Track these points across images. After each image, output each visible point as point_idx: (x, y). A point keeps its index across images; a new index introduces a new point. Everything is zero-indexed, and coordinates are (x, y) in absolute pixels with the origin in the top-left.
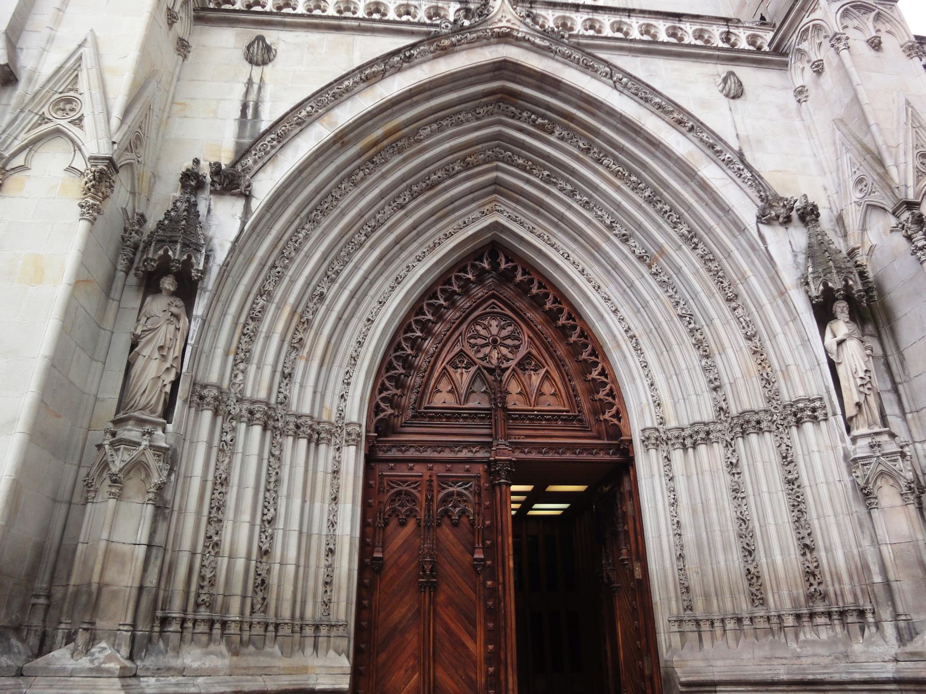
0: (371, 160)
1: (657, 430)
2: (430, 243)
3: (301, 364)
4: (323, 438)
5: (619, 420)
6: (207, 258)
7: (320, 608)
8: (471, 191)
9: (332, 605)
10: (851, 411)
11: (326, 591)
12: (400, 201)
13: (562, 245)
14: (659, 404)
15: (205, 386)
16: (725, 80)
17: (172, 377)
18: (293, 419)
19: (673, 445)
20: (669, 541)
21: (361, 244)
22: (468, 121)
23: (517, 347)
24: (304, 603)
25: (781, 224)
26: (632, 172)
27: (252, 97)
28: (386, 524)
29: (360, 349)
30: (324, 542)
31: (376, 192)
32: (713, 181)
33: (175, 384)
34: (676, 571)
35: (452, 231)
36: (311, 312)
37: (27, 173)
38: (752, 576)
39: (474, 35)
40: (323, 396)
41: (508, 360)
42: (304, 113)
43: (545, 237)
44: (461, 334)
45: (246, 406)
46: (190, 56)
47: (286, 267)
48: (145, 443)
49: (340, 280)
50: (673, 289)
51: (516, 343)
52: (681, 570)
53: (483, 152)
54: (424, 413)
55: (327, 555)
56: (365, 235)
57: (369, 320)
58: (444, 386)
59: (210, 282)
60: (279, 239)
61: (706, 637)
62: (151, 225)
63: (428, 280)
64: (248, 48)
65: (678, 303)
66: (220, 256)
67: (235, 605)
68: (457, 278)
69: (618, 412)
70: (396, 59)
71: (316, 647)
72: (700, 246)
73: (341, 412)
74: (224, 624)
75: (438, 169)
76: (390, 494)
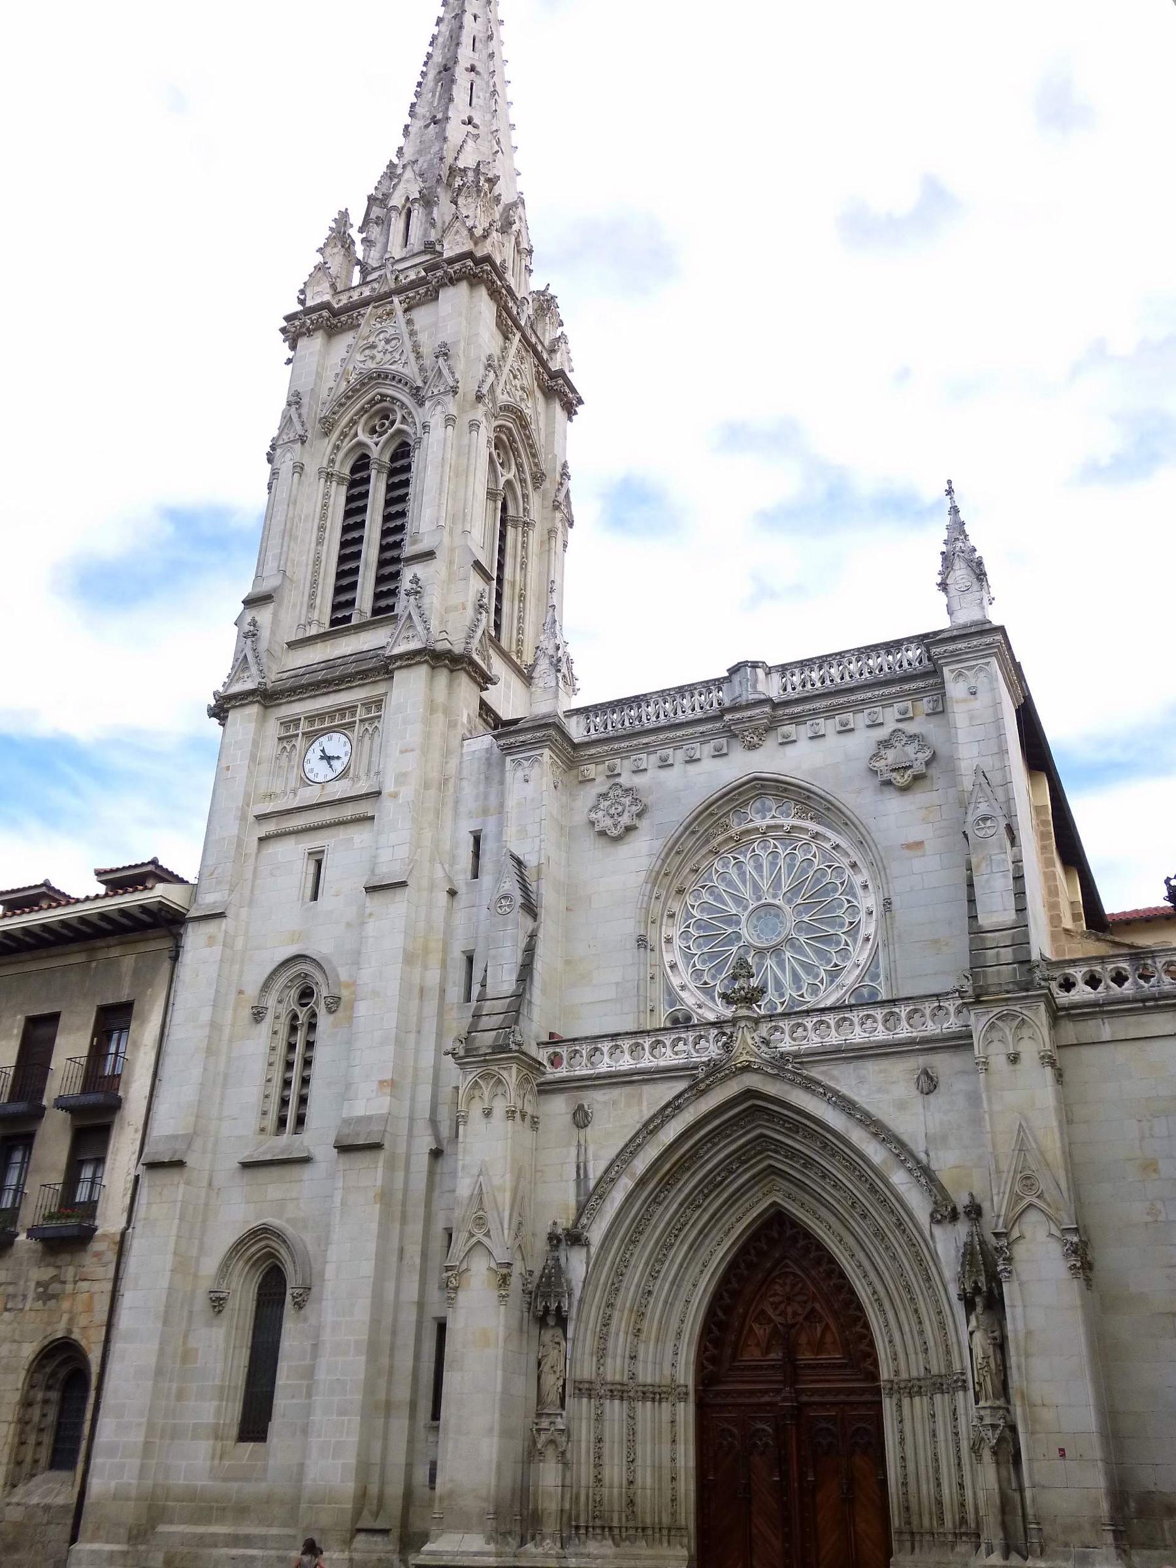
0: (667, 1183)
1: (892, 1382)
2: (727, 1227)
3: (642, 1347)
6: (570, 1295)
8: (753, 1177)
12: (697, 1203)
15: (581, 1382)
17: (561, 1382)
18: (641, 1388)
20: (896, 1473)
22: (736, 1131)
23: (805, 1302)
25: (950, 1222)
26: (855, 1168)
31: (675, 1206)
32: (900, 1186)
33: (564, 1386)
35: (741, 1215)
37: (469, 1273)
38: (940, 1503)
39: (723, 1074)
40: (661, 1364)
41: (799, 1315)
42: (613, 1173)
45: (609, 1387)
46: (540, 1126)
47: (621, 1281)
49: (662, 1274)
51: (805, 1298)
53: (753, 1148)
61: (917, 1545)
62: (537, 1274)
64: (574, 1114)
66: (577, 1293)
67: (616, 1516)
70: (670, 1110)
71: (669, 1542)
74: (611, 1528)
75: (722, 1170)
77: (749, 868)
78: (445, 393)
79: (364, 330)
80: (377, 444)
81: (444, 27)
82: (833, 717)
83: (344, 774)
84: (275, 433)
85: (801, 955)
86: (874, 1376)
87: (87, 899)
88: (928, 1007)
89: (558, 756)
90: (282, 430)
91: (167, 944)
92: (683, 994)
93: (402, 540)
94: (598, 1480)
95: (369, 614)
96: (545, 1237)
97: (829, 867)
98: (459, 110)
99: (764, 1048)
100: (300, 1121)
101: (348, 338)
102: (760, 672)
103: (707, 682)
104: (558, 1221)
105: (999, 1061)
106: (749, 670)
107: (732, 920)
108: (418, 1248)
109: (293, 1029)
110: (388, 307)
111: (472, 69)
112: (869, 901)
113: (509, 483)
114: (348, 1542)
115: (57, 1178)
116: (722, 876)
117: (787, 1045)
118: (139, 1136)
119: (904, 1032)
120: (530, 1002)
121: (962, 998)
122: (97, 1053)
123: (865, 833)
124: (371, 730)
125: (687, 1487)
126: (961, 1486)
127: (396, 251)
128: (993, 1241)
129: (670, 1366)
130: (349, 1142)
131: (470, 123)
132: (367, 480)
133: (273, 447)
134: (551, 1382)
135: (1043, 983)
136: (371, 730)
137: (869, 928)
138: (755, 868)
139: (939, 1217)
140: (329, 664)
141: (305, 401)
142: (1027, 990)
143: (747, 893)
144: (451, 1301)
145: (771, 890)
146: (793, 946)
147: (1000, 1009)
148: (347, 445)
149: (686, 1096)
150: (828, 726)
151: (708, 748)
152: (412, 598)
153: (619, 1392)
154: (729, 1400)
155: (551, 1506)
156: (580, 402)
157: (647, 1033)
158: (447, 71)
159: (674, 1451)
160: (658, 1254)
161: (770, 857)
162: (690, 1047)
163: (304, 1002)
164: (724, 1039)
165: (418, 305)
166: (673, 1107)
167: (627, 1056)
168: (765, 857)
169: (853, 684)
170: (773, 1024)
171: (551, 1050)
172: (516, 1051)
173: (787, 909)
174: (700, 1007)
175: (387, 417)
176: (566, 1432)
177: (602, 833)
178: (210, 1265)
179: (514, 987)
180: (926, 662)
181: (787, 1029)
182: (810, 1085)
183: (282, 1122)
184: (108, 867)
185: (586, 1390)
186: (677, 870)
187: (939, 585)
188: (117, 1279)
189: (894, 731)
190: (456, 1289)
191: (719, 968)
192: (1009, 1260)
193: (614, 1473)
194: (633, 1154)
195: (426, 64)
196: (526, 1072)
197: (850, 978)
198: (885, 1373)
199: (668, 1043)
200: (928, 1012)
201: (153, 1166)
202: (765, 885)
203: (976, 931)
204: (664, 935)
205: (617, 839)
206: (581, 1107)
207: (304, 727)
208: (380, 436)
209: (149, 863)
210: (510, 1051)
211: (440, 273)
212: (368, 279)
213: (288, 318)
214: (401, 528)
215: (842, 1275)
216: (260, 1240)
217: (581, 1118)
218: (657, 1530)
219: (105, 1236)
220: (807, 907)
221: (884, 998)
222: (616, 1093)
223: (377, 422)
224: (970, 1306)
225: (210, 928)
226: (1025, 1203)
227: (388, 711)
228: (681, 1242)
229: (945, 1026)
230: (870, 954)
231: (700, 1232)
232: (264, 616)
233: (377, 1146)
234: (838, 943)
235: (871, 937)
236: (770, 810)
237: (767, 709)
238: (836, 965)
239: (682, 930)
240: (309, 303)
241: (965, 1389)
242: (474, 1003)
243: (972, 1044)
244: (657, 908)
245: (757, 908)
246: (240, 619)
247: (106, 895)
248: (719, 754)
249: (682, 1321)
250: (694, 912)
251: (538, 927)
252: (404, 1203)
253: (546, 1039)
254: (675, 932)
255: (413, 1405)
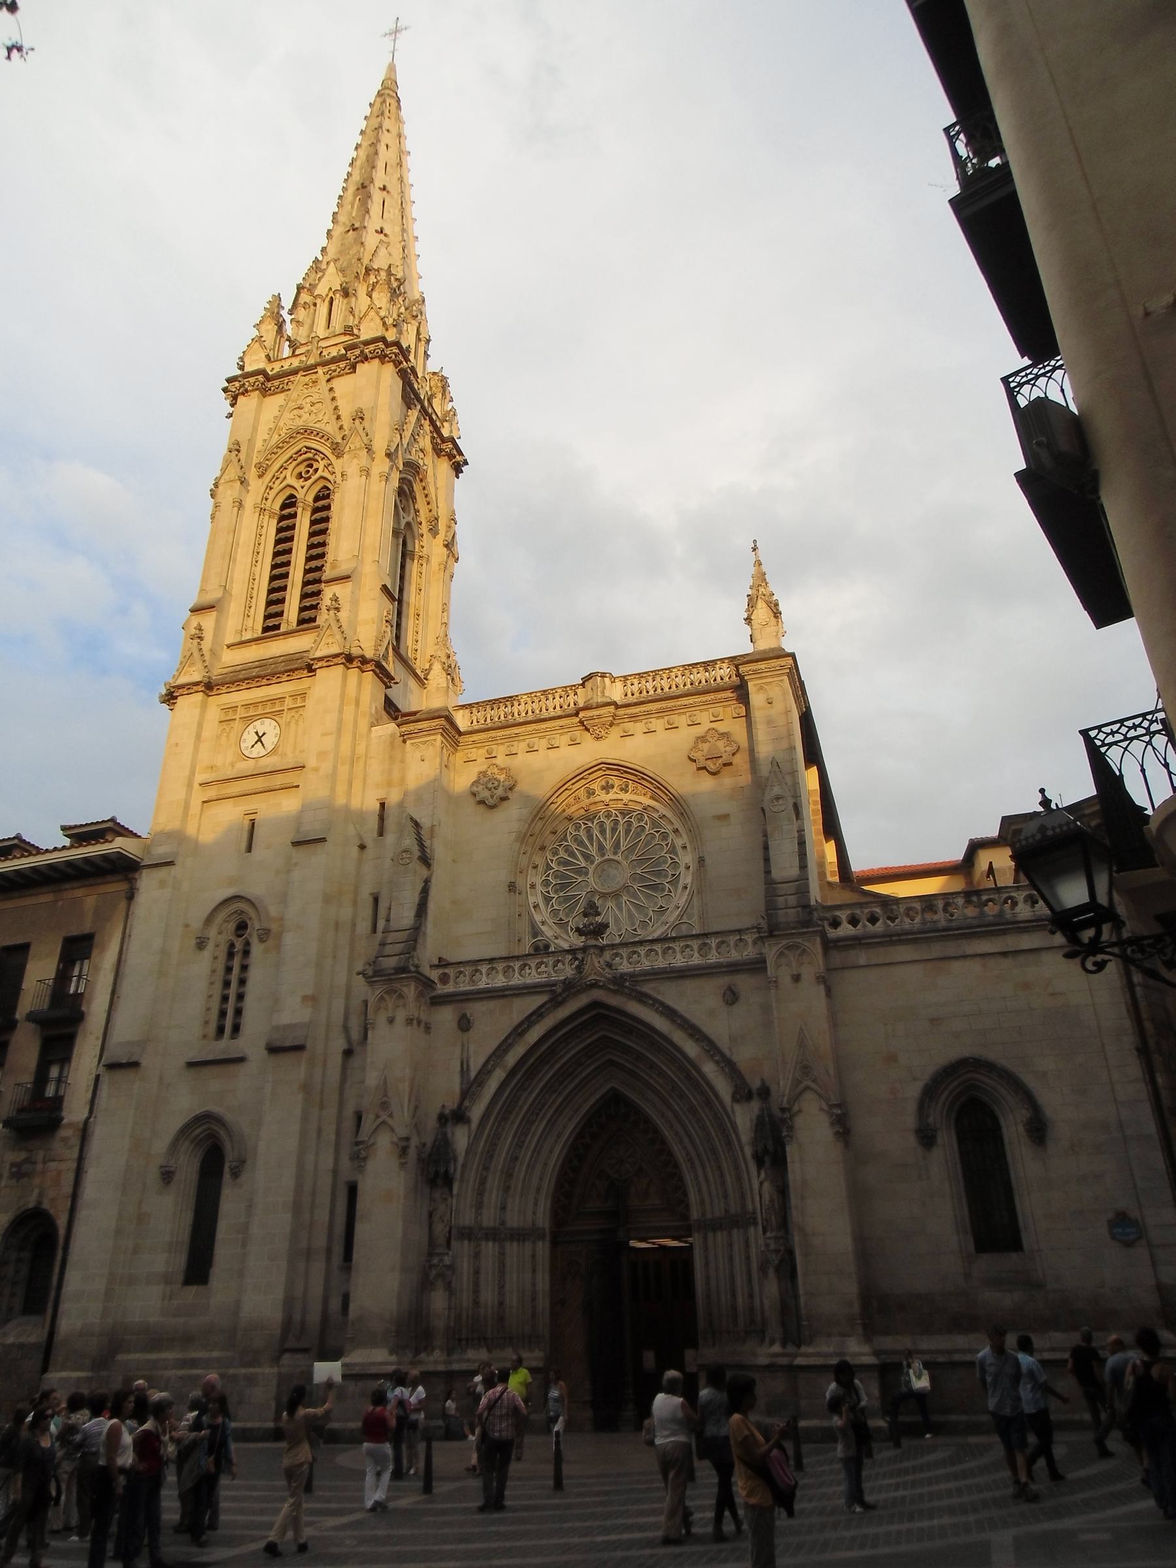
10: (765, 1224)
16: (724, 993)
17: (448, 1229)
27: (465, 1055)
31: (537, 1091)
33: (450, 1232)
38: (734, 1308)
48: (441, 1265)
49: (526, 1144)
59: (458, 1176)
60: (489, 1135)
62: (429, 1145)
64: (459, 1021)
73: (533, 1222)
77: (596, 832)
78: (360, 448)
79: (294, 394)
80: (302, 488)
81: (363, 153)
82: (662, 717)
83: (274, 751)
84: (218, 474)
85: (634, 899)
86: (685, 1217)
87: (55, 849)
88: (733, 939)
89: (447, 741)
90: (223, 471)
91: (123, 886)
92: (544, 928)
93: (323, 566)
94: (476, 1303)
95: (295, 624)
96: (435, 1117)
97: (658, 832)
98: (373, 222)
99: (607, 970)
100: (236, 1029)
101: (279, 399)
102: (607, 680)
103: (565, 687)
104: (446, 1104)
105: (786, 980)
106: (599, 679)
107: (582, 871)
108: (333, 1127)
109: (231, 955)
110: (314, 377)
111: (384, 188)
112: (687, 858)
113: (408, 525)
114: (276, 1360)
115: (27, 1078)
116: (577, 840)
117: (625, 967)
118: (100, 1042)
119: (713, 958)
120: (425, 934)
121: (759, 932)
122: (63, 977)
123: (685, 807)
124: (296, 717)
125: (543, 1303)
126: (751, 1296)
127: (321, 331)
128: (778, 1113)
130: (278, 1044)
131: (382, 232)
132: (294, 516)
133: (216, 485)
134: (440, 1229)
135: (819, 922)
136: (296, 717)
137: (687, 879)
138: (600, 831)
139: (738, 1097)
140: (262, 663)
141: (243, 449)
142: (808, 927)
143: (593, 850)
144: (361, 1169)
145: (612, 849)
146: (628, 892)
147: (787, 941)
148: (277, 487)
149: (547, 1006)
150: (658, 724)
151: (566, 739)
152: (332, 612)
153: (493, 1234)
155: (439, 1324)
156: (466, 463)
157: (517, 958)
158: (364, 188)
161: (612, 824)
162: (550, 969)
163: (239, 933)
164: (577, 963)
165: (339, 376)
166: (537, 1015)
167: (501, 976)
168: (608, 824)
169: (678, 692)
170: (615, 951)
171: (441, 971)
172: (414, 972)
173: (624, 863)
174: (556, 938)
175: (311, 466)
176: (451, 1267)
177: (482, 802)
178: (161, 1145)
179: (412, 922)
180: (734, 678)
181: (625, 955)
182: (642, 998)
183: (221, 1030)
184: (72, 824)
185: (467, 1234)
186: (540, 832)
187: (745, 620)
188: (81, 1159)
189: (709, 729)
190: (365, 1159)
191: (571, 909)
192: (791, 1128)
193: (488, 1296)
194: (506, 1051)
195: (346, 181)
196: (421, 988)
197: (672, 917)
198: (695, 1214)
199: (533, 965)
200: (732, 943)
201: (113, 1067)
202: (608, 845)
203: (770, 884)
204: (529, 883)
205: (492, 807)
206: (464, 1016)
207: (241, 712)
208: (306, 479)
209: (108, 821)
210: (410, 972)
211: (357, 352)
212: (297, 353)
213: (229, 380)
214: (322, 556)
215: (663, 1142)
216: (204, 1124)
217: (464, 1024)
219: (70, 1125)
220: (640, 861)
221: (698, 932)
222: (492, 1004)
223: (302, 468)
224: (760, 1162)
225: (162, 873)
226: (802, 1086)
227: (309, 703)
229: (745, 953)
230: (687, 899)
232: (208, 621)
233: (299, 1048)
234: (663, 890)
235: (689, 886)
236: (613, 787)
237: (612, 709)
238: (661, 907)
239: (543, 878)
240: (248, 369)
241: (755, 1224)
242: (379, 934)
243: (766, 968)
244: (524, 861)
245: (601, 863)
246: (188, 622)
247: (72, 847)
248: (574, 743)
249: (541, 1179)
250: (553, 865)
251: (431, 875)
252: (322, 1093)
253: (436, 962)
254: (538, 881)
255: (329, 1251)
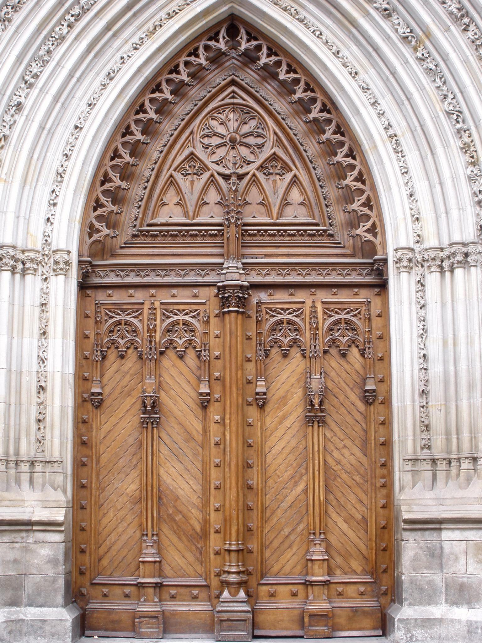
1: (412, 250)
2: (150, 26)
4: (28, 269)
5: (375, 235)
7: (34, 445)
9: (46, 442)
11: (39, 429)
13: (313, 20)
14: (417, 219)
19: (429, 267)
21: (64, 38)
24: (18, 441)
28: (104, 357)
29: (67, 163)
30: (35, 379)
34: (417, 407)
35: (176, 9)
36: (8, 127)
40: (28, 221)
43: (293, 10)
44: (191, 133)
50: (441, 78)
51: (260, 141)
52: (423, 407)
54: (148, 231)
55: (39, 393)
56: (69, 26)
57: (76, 127)
58: (171, 197)
61: (441, 475)
63: (148, 71)
65: (445, 97)
68: (187, 64)
69: (374, 226)
71: (31, 481)
72: (472, 27)
76: (108, 324)
129: (42, 220)
154: (132, 279)
159: (43, 348)
160: (39, 48)
218: (12, 465)
228: (76, 39)
231: (108, 27)
